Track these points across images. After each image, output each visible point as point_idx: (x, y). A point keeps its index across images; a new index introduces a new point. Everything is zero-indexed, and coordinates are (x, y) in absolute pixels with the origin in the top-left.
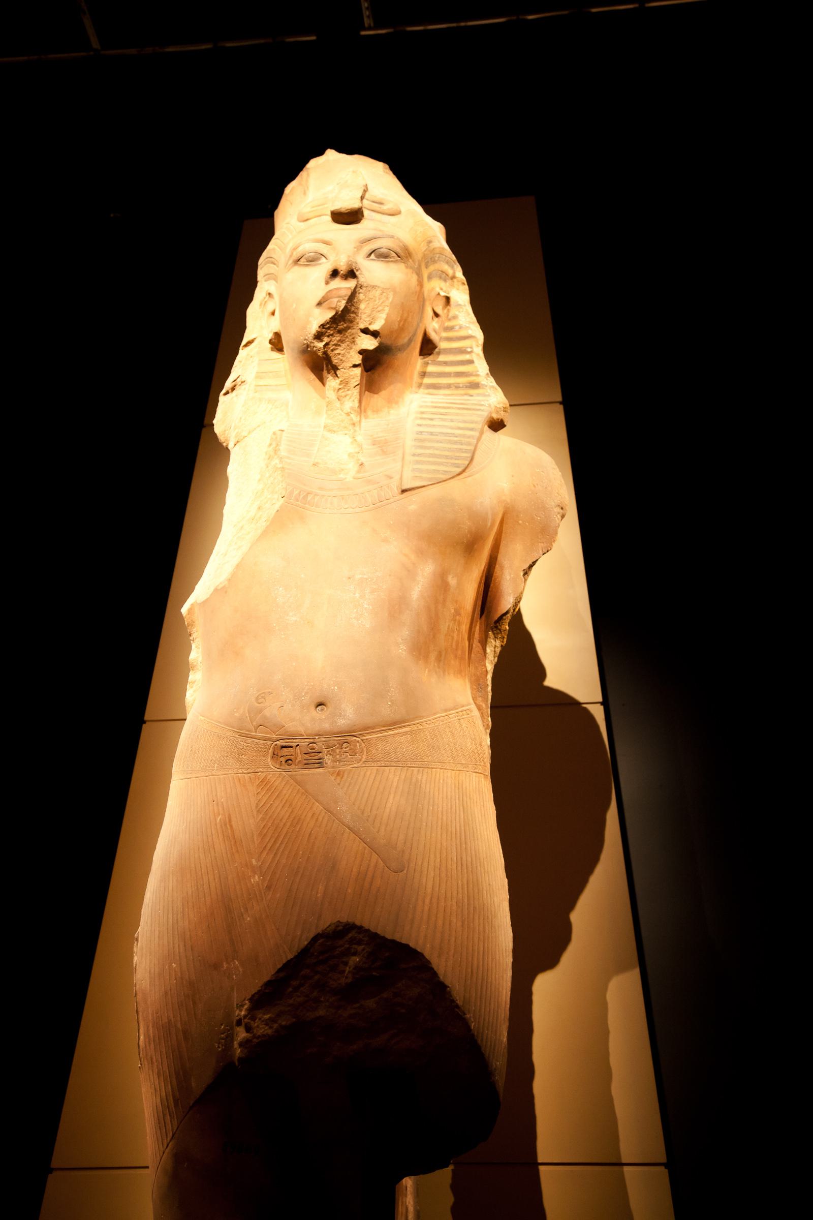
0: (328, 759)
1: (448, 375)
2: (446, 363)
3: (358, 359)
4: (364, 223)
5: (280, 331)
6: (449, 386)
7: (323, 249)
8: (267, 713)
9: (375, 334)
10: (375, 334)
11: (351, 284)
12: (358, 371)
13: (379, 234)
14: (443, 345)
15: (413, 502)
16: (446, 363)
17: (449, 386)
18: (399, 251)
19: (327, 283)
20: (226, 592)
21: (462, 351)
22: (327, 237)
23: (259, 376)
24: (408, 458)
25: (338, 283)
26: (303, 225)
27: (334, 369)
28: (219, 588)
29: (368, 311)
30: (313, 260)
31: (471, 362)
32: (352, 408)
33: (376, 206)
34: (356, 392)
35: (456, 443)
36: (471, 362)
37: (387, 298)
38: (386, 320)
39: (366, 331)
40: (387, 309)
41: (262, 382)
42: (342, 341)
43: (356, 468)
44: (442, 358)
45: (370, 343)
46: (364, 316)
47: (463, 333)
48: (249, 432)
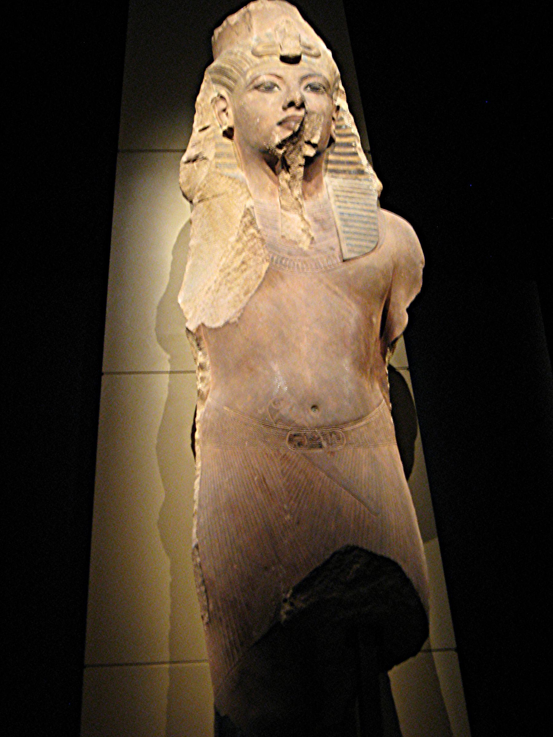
0: (324, 444)
1: (342, 163)
2: (339, 154)
3: (302, 162)
4: (302, 63)
5: (234, 127)
6: (344, 172)
7: (277, 82)
8: (283, 412)
9: (314, 146)
10: (314, 146)
11: (301, 113)
12: (302, 169)
13: (312, 73)
14: (337, 140)
15: (351, 269)
16: (339, 154)
17: (344, 172)
18: (324, 85)
19: (284, 109)
20: (237, 326)
21: (349, 145)
22: (279, 73)
23: (217, 156)
24: (342, 235)
25: (292, 111)
26: (257, 60)
27: (287, 168)
28: (231, 321)
29: (310, 129)
30: (270, 88)
31: (355, 154)
32: (299, 195)
33: (307, 51)
34: (300, 183)
35: (366, 223)
36: (355, 154)
37: (320, 120)
38: (321, 137)
39: (309, 143)
40: (321, 128)
41: (220, 161)
42: (294, 149)
43: (309, 241)
44: (337, 150)
45: (310, 152)
46: (307, 133)
47: (348, 132)
48: (213, 196)
